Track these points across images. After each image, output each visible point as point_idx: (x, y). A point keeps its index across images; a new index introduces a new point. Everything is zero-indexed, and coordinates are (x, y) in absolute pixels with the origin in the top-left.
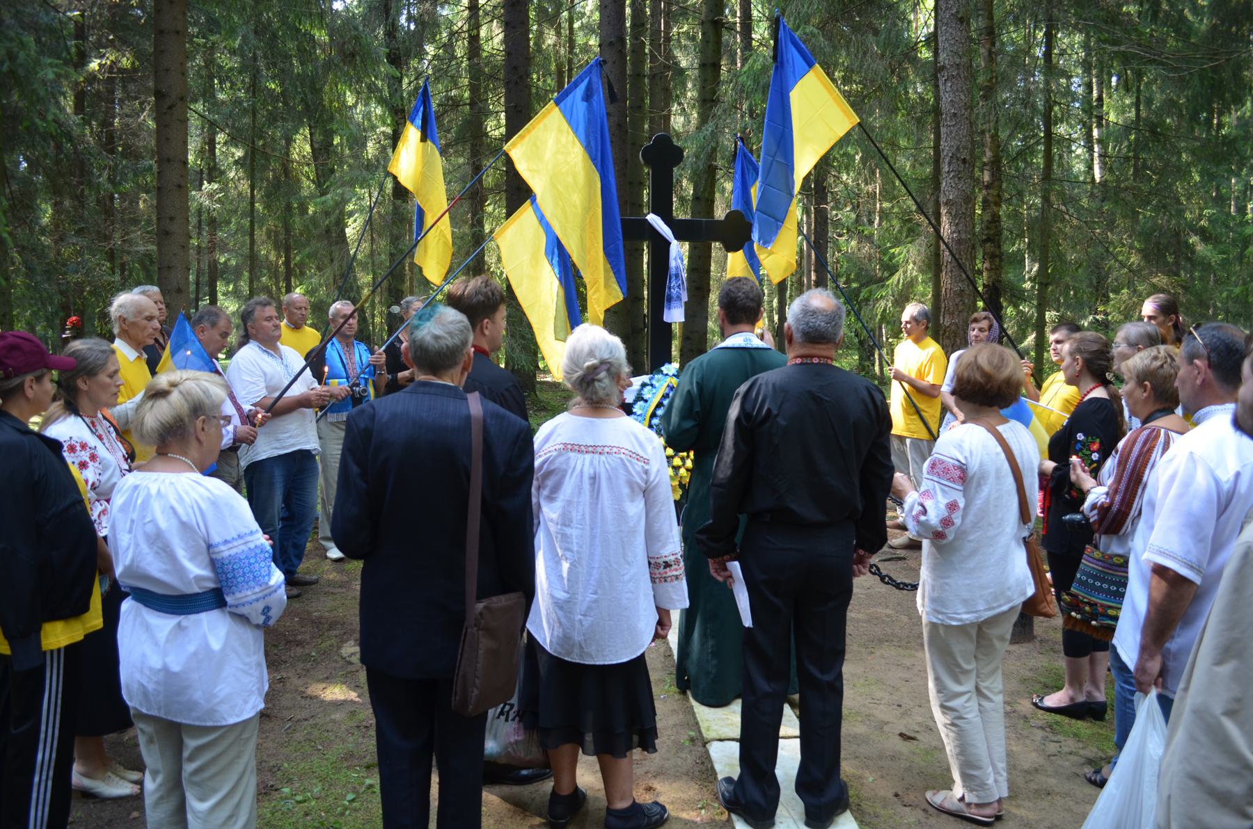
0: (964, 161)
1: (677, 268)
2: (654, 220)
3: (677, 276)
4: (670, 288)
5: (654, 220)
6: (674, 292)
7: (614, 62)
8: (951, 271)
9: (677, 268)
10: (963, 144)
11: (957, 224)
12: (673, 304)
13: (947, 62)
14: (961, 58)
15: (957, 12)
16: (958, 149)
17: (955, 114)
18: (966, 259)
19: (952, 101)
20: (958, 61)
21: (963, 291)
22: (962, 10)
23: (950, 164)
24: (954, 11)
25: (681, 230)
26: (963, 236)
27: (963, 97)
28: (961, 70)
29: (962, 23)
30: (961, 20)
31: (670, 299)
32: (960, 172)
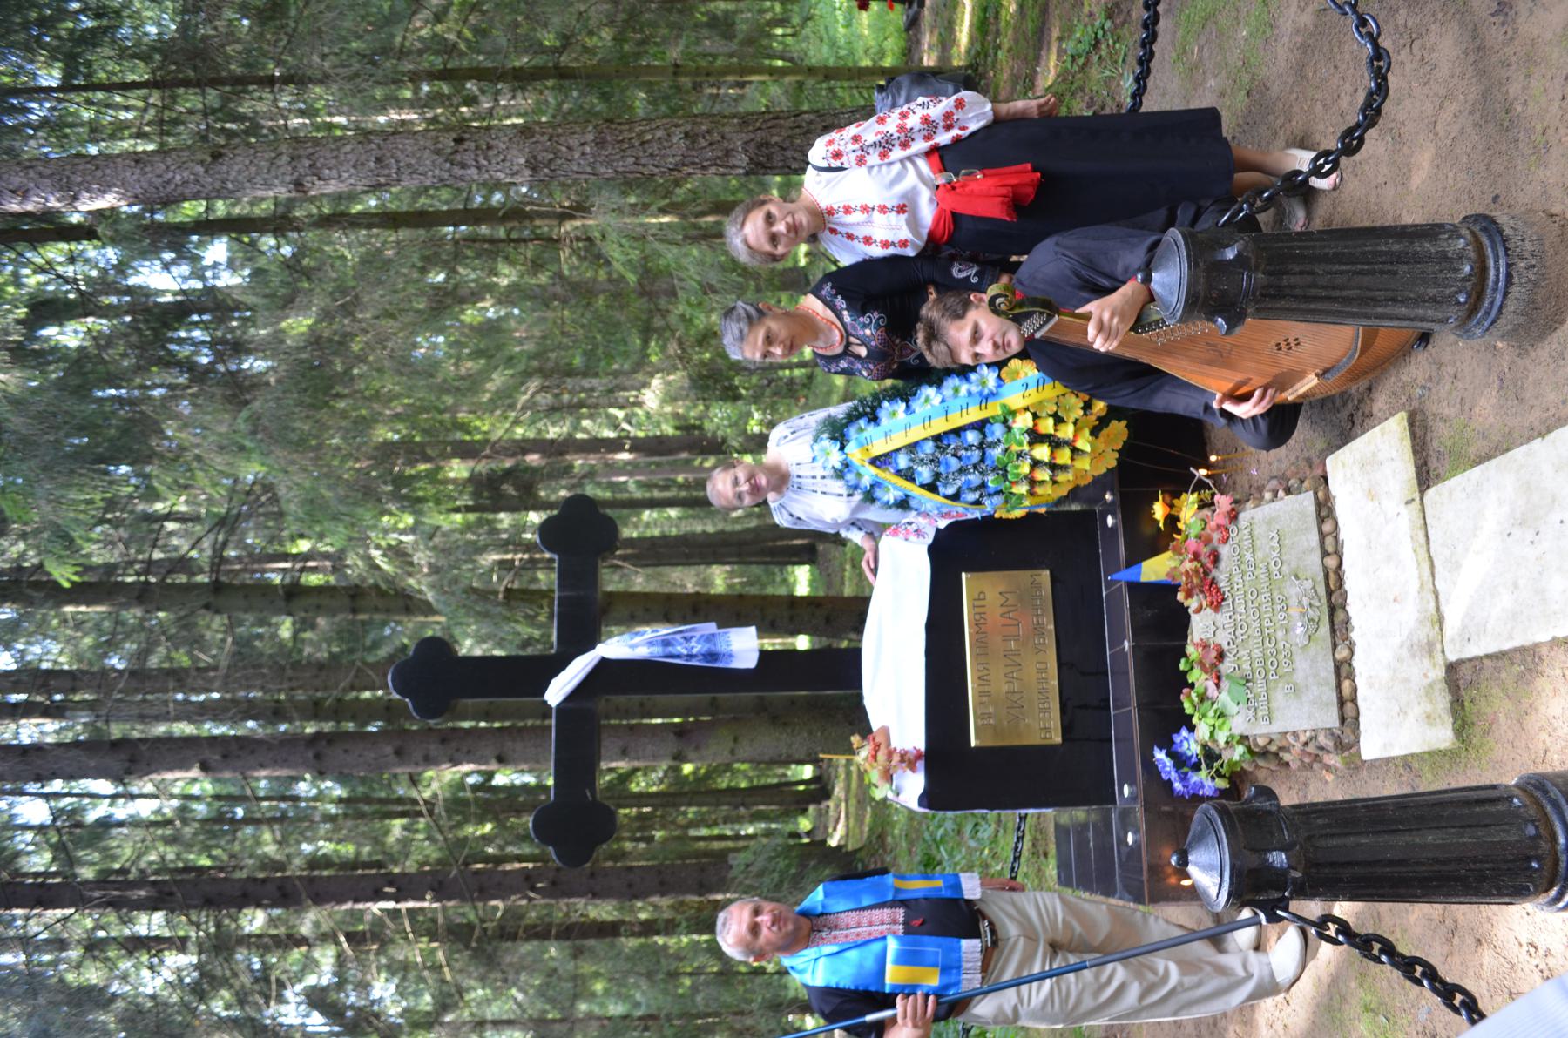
0: (459, 141)
1: (650, 643)
2: (557, 691)
3: (666, 643)
4: (691, 656)
5: (557, 691)
6: (697, 648)
7: (346, 751)
8: (652, 155)
9: (650, 643)
10: (429, 143)
11: (570, 148)
12: (721, 648)
13: (288, 178)
14: (281, 154)
15: (202, 163)
16: (438, 152)
17: (378, 160)
18: (630, 130)
19: (354, 167)
20: (285, 159)
21: (686, 135)
22: (199, 156)
23: (464, 166)
24: (200, 169)
25: (579, 637)
26: (591, 137)
27: (348, 148)
28: (302, 152)
29: (221, 155)
30: (217, 156)
31: (712, 656)
32: (477, 148)
